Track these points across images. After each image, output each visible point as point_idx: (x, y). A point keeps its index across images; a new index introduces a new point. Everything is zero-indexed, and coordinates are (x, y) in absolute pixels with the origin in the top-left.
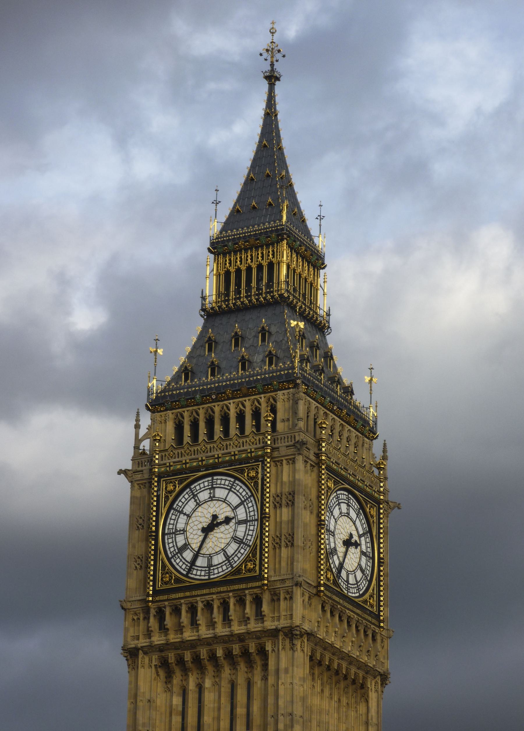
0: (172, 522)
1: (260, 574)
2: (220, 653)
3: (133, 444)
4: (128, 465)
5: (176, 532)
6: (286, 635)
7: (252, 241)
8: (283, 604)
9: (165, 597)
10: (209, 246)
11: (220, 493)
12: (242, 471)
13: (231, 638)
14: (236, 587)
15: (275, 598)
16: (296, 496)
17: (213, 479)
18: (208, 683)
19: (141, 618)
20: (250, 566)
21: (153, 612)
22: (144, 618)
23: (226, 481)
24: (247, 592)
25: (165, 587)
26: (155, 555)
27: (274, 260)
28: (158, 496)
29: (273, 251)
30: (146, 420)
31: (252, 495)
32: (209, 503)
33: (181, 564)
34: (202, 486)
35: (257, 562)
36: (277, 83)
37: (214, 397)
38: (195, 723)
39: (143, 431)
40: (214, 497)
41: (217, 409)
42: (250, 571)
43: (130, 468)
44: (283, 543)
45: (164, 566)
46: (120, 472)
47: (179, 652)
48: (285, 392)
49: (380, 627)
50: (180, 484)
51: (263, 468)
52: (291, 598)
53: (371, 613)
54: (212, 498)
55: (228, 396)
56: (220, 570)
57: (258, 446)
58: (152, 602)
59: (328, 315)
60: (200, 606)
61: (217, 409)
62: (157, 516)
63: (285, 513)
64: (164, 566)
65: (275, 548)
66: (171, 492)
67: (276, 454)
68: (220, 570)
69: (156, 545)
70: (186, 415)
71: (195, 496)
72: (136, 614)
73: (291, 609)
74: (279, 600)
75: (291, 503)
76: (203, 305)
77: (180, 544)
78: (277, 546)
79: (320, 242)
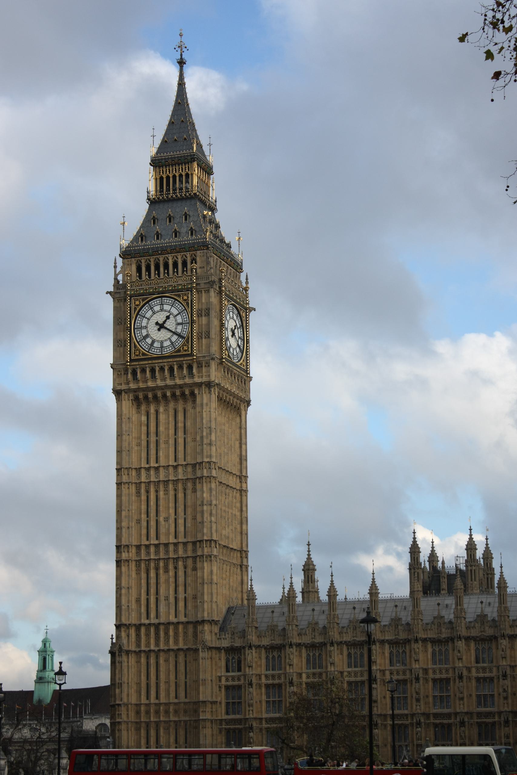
0: (139, 322)
1: (192, 353)
2: (168, 394)
4: (112, 289)
5: (141, 328)
6: (206, 385)
9: (137, 363)
10: (150, 162)
12: (179, 296)
13: (175, 386)
14: (178, 359)
16: (210, 311)
18: (161, 409)
20: (185, 348)
21: (130, 371)
22: (124, 374)
23: (170, 301)
24: (184, 362)
26: (130, 340)
27: (190, 173)
28: (130, 308)
29: (188, 167)
30: (120, 262)
31: (185, 309)
33: (145, 345)
34: (156, 303)
35: (190, 346)
36: (184, 65)
38: (155, 431)
39: (118, 269)
41: (161, 259)
42: (185, 351)
43: (112, 290)
44: (203, 336)
46: (107, 293)
49: (247, 377)
50: (143, 301)
51: (191, 295)
52: (209, 366)
53: (243, 370)
54: (162, 310)
56: (168, 349)
57: (189, 282)
58: (129, 365)
59: (216, 201)
60: (157, 369)
61: (161, 259)
62: (130, 318)
63: (204, 320)
65: (198, 339)
66: (138, 305)
67: (198, 287)
68: (168, 349)
69: (130, 334)
70: (143, 261)
71: (151, 308)
72: (119, 371)
73: (208, 372)
74: (202, 367)
75: (208, 314)
76: (148, 196)
77: (144, 334)
78: (200, 338)
79: (210, 159)
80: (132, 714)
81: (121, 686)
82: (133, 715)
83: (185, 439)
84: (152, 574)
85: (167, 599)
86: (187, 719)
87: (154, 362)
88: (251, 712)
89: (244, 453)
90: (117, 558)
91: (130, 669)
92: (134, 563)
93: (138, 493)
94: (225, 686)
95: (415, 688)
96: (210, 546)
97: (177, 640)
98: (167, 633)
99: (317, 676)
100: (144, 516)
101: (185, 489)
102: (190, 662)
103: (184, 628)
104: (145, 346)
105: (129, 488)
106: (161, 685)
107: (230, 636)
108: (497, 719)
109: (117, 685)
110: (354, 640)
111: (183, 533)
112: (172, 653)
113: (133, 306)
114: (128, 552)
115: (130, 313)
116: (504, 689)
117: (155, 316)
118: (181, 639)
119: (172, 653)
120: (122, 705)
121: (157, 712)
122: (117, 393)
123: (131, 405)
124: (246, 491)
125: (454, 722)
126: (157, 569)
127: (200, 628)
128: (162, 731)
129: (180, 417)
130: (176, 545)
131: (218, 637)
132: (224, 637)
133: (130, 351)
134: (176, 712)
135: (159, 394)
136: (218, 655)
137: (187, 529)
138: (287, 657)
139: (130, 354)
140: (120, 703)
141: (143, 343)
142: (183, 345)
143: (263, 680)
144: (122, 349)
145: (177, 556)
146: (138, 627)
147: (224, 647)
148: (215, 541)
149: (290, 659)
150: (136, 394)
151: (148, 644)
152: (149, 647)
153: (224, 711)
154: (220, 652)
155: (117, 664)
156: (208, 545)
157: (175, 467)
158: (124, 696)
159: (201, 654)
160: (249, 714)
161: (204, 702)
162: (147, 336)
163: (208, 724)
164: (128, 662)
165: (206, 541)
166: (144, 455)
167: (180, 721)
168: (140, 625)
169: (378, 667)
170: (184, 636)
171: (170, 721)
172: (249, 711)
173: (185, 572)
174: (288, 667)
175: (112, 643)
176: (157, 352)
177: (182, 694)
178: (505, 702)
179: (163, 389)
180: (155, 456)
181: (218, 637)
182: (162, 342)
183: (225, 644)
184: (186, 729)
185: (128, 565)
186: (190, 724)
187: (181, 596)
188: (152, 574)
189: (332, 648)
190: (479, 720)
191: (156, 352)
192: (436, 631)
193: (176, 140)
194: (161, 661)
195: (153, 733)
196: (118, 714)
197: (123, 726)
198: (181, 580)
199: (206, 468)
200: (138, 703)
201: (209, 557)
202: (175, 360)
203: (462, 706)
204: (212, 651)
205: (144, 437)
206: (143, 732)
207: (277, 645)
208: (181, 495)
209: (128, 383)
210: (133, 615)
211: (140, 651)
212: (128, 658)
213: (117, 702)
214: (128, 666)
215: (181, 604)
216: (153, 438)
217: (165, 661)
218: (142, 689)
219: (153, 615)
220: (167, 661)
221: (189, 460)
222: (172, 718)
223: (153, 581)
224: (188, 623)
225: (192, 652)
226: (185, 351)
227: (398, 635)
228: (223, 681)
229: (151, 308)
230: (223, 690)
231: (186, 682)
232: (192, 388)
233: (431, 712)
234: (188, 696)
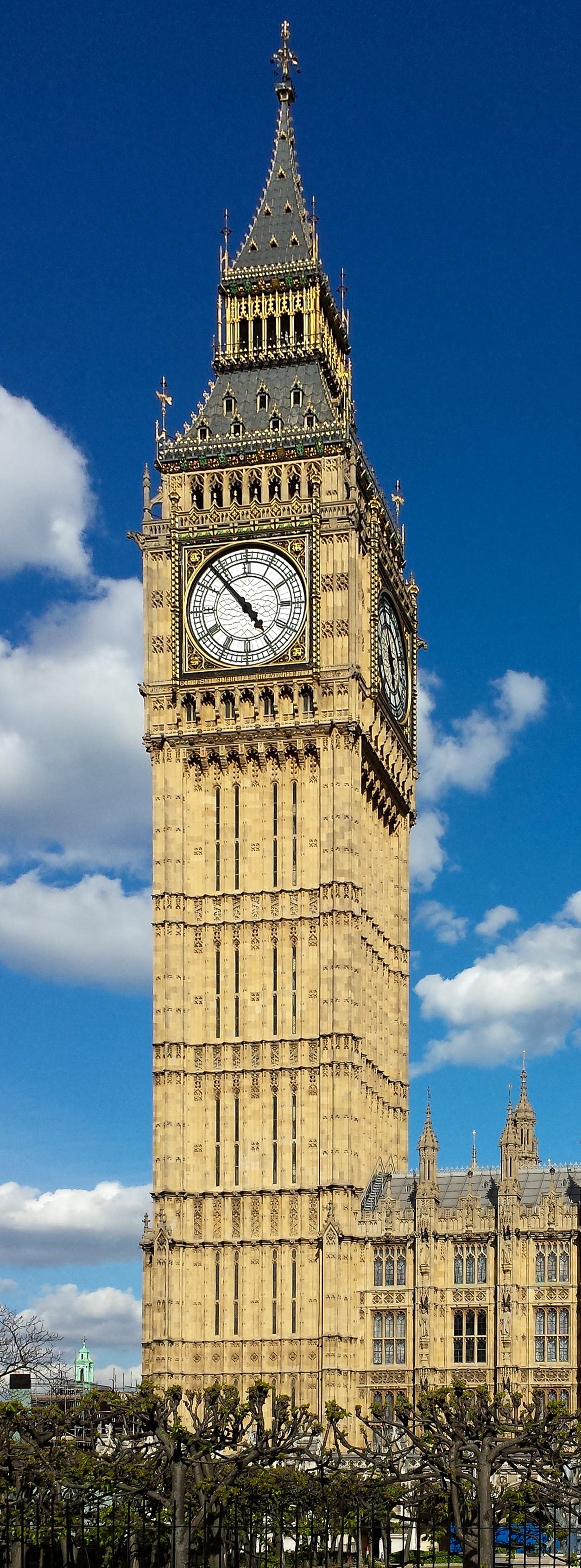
2: (261, 749)
9: (194, 682)
11: (257, 569)
17: (247, 552)
32: (243, 579)
33: (212, 647)
34: (234, 559)
37: (242, 458)
40: (249, 573)
45: (191, 648)
55: (259, 457)
64: (191, 648)
66: (195, 563)
69: (181, 622)
77: (209, 626)
83: (295, 841)
101: (294, 939)
112: (267, 1248)
126: (237, 1091)
129: (285, 796)
130: (274, 1044)
135: (242, 749)
136: (358, 1253)
141: (208, 643)
151: (217, 1230)
153: (369, 1356)
162: (216, 628)
173: (294, 1098)
176: (238, 662)
179: (250, 739)
185: (179, 1082)
187: (285, 1142)
191: (235, 662)
194: (245, 1261)
208: (285, 950)
215: (285, 1158)
219: (228, 1178)
223: (228, 1114)
231: (294, 1303)
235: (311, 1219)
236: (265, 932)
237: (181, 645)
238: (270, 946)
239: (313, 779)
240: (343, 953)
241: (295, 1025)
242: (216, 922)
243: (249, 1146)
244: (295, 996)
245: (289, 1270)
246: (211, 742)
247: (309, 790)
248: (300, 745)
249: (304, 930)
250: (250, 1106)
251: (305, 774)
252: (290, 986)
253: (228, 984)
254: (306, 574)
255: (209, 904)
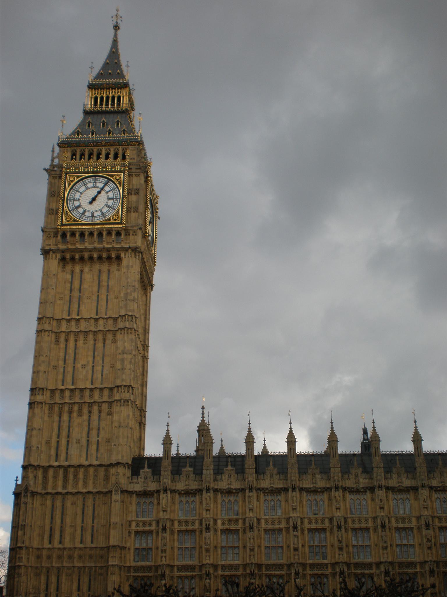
2: (95, 256)
3: (50, 158)
5: (74, 200)
6: (133, 250)
7: (111, 85)
8: (132, 237)
9: (68, 227)
12: (112, 176)
14: (108, 226)
15: (127, 233)
19: (52, 236)
20: (115, 218)
22: (54, 237)
25: (67, 223)
30: (57, 149)
31: (117, 187)
35: (120, 217)
39: (55, 154)
42: (115, 220)
44: (132, 210)
45: (67, 213)
47: (73, 254)
48: (133, 147)
50: (78, 177)
51: (124, 176)
54: (95, 186)
60: (87, 234)
62: (64, 191)
63: (134, 198)
66: (72, 181)
67: (130, 171)
69: (63, 203)
72: (49, 234)
74: (129, 235)
78: (128, 211)
80: (32, 558)
81: (25, 528)
82: (33, 559)
83: (107, 295)
84: (65, 417)
85: (78, 442)
86: (93, 565)
87: (84, 227)
88: (164, 558)
89: (147, 327)
90: (30, 400)
91: (34, 511)
92: (47, 406)
93: (57, 341)
94: (135, 532)
95: (338, 536)
96: (128, 392)
97: (86, 483)
98: (76, 476)
99: (233, 522)
100: (61, 363)
101: (104, 340)
102: (99, 506)
103: (95, 471)
104: (76, 215)
105: (49, 336)
106: (67, 528)
107: (143, 480)
108: (418, 569)
109: (20, 526)
110: (272, 487)
111: (100, 380)
113: (67, 181)
114: (43, 394)
115: (65, 186)
116: (428, 539)
117: (87, 191)
118: (91, 482)
119: (80, 497)
120: (24, 548)
121: (59, 557)
122: (45, 252)
123: (57, 263)
124: (147, 358)
125: (376, 572)
126: (70, 412)
127: (113, 471)
128: (64, 578)
129: (104, 277)
130: (91, 390)
131: (130, 481)
132: (136, 481)
133: (62, 217)
134: (80, 557)
135: (86, 255)
137: (104, 376)
138: (204, 502)
139: (62, 219)
140: (23, 545)
142: (113, 216)
143: (176, 526)
144: (53, 217)
145: (92, 401)
146: (46, 469)
147: (136, 491)
148: (132, 388)
149: (207, 504)
150: (63, 254)
151: (55, 486)
152: (56, 489)
154: (131, 496)
155: (22, 505)
156: (126, 391)
157: (96, 320)
158: (26, 538)
159: (114, 497)
160: (161, 561)
161: (114, 546)
162: (79, 207)
163: (117, 570)
164: (33, 504)
165: (125, 386)
166: (66, 308)
167: (85, 567)
168: (50, 467)
169: (299, 515)
170: (94, 479)
171: (74, 567)
172: (162, 557)
173: (100, 416)
174: (204, 512)
175: (17, 485)
177: (89, 539)
178: (429, 551)
180: (77, 310)
181: (130, 481)
182: (93, 213)
183: (138, 487)
184: (90, 576)
185: (42, 408)
186: (95, 571)
187: (94, 438)
188: (65, 417)
189: (251, 494)
190: (400, 571)
192: (354, 481)
193: (110, 73)
194: (68, 504)
195: (53, 579)
196: (19, 557)
197: (22, 571)
198: (95, 423)
199: (128, 321)
200: (40, 547)
201: (126, 402)
202: (105, 226)
203: (386, 556)
204: (124, 495)
205: (67, 292)
206: (43, 578)
207: (192, 490)
208: (100, 345)
209: (57, 245)
210: (42, 457)
211: (47, 493)
212: (33, 500)
213: (19, 545)
214: (33, 508)
215: (94, 447)
216: (76, 294)
217: (72, 504)
218: (46, 532)
219: (62, 457)
220: (73, 504)
221: (110, 314)
222: (77, 564)
223: (65, 424)
224: (100, 465)
225: (102, 495)
226: (115, 220)
227: (316, 483)
228: (134, 527)
229: (85, 185)
230: (133, 535)
231: (93, 526)
232: (120, 252)
233: (352, 562)
234: (95, 541)
235: (104, 480)
236: (91, 336)
237: (63, 212)
238: (92, 342)
239: (118, 270)
240: (128, 346)
241: (102, 380)
242: (67, 331)
243: (75, 441)
244: (103, 366)
245: (91, 508)
246: (72, 252)
247: (115, 273)
248: (113, 255)
249: (110, 336)
250: (76, 420)
251: (114, 267)
252: (101, 362)
253: (70, 361)
254: (121, 189)
255: (64, 322)
